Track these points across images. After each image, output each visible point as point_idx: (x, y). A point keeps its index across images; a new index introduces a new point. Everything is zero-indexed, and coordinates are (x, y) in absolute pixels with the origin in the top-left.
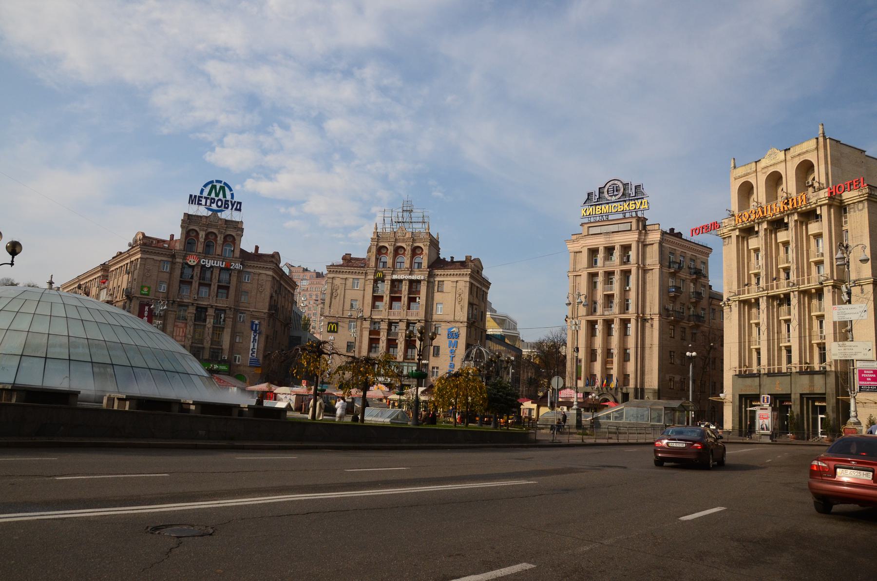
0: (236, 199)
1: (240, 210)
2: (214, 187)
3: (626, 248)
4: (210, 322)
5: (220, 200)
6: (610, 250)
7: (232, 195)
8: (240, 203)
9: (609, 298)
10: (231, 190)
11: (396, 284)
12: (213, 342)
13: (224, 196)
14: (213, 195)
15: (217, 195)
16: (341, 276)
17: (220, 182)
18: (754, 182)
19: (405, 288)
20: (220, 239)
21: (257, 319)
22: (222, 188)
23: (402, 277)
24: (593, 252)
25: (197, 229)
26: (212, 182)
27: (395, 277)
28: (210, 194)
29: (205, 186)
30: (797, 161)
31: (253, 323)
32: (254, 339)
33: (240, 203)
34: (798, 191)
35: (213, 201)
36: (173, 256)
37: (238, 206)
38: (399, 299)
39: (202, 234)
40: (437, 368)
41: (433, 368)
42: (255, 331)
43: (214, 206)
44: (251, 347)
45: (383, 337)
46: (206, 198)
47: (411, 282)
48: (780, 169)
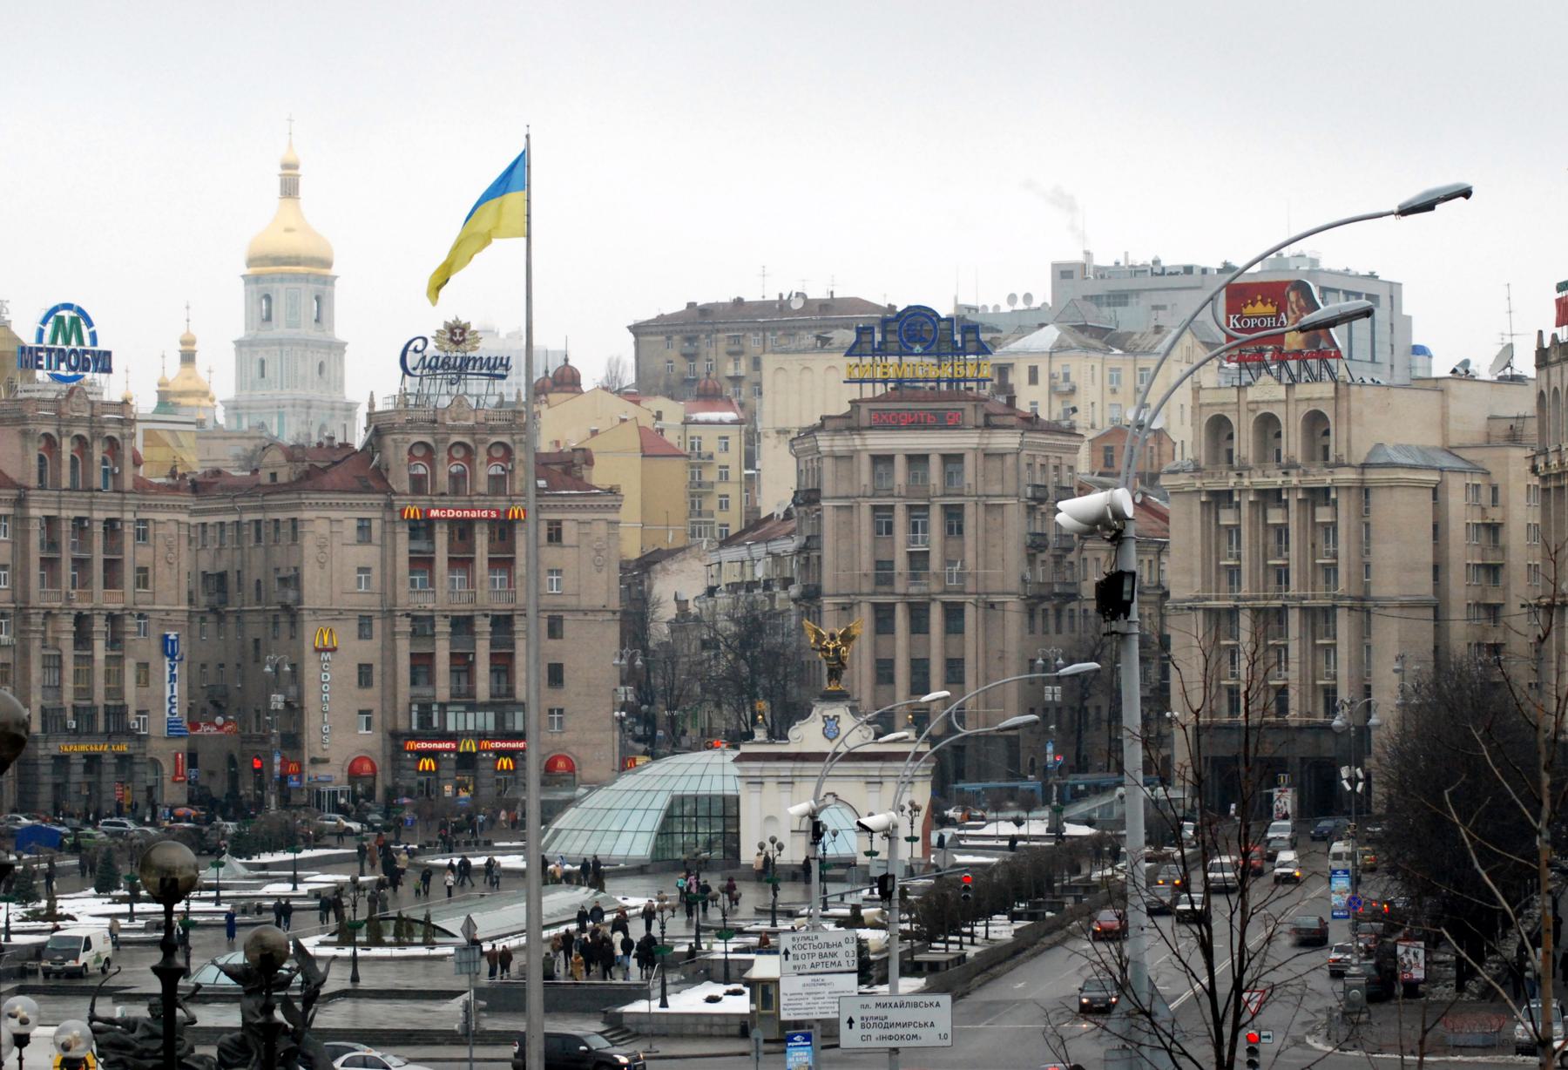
0: (102, 346)
1: (108, 370)
2: (60, 320)
3: (952, 460)
5: (74, 351)
7: (93, 336)
8: (108, 354)
9: (918, 561)
10: (90, 324)
12: (109, 693)
13: (81, 342)
14: (60, 344)
15: (68, 342)
16: (334, 515)
17: (68, 307)
18: (1233, 419)
19: (482, 541)
20: (98, 451)
21: (172, 628)
22: (74, 321)
24: (882, 460)
25: (51, 430)
26: (56, 309)
28: (54, 341)
29: (44, 322)
30: (1304, 409)
31: (166, 637)
32: (173, 677)
33: (108, 354)
35: (62, 356)
36: (21, 502)
37: (103, 362)
39: (67, 448)
40: (560, 711)
41: (551, 711)
42: (172, 659)
43: (63, 370)
44: (168, 694)
46: (50, 351)
48: (1278, 411)
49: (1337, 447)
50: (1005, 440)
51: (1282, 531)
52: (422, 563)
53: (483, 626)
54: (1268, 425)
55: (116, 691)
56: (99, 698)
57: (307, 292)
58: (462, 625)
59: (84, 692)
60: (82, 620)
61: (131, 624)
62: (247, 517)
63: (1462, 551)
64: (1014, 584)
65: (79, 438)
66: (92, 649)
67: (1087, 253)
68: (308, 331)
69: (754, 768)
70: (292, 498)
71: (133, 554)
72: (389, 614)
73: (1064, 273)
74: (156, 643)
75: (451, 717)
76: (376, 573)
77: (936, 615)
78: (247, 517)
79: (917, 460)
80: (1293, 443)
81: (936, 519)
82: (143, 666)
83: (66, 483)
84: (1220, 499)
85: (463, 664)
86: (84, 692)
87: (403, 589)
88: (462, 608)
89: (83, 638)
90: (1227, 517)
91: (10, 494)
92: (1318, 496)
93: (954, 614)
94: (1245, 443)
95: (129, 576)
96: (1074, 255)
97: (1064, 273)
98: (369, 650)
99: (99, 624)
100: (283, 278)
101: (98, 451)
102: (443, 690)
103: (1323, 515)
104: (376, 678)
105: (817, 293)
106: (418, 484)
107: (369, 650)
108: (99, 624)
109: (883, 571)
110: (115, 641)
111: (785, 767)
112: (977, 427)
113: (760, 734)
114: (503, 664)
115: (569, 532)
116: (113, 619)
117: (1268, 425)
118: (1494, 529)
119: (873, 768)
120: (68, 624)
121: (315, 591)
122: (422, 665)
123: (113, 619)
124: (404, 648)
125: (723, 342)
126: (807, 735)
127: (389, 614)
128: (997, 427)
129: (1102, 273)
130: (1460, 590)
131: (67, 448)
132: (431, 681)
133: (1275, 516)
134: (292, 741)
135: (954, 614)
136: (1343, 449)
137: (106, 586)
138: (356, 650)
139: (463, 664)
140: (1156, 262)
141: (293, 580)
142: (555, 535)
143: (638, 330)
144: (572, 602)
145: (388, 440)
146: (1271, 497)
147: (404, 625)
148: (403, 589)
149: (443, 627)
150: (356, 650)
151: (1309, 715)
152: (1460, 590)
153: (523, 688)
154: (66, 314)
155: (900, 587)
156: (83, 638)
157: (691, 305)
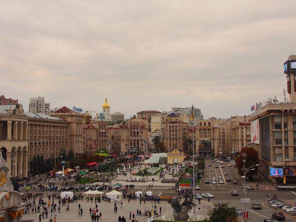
3: (176, 126)
4: (104, 142)
6: (173, 126)
9: (173, 135)
11: (134, 132)
18: (202, 123)
19: (136, 133)
20: (104, 125)
23: (136, 131)
24: (170, 126)
27: (134, 131)
30: (209, 122)
34: (209, 126)
35: (101, 117)
36: (97, 130)
38: (135, 135)
39: (101, 125)
45: (133, 143)
47: (137, 132)
49: (211, 125)
50: (181, 124)
51: (206, 132)
52: (131, 135)
53: (136, 141)
54: (205, 124)
55: (105, 147)
56: (104, 147)
57: (108, 110)
58: (134, 140)
59: (103, 147)
60: (103, 140)
61: (106, 141)
62: (116, 131)
63: (221, 134)
64: (181, 137)
65: (102, 125)
68: (108, 113)
69: (169, 155)
70: (119, 130)
71: (107, 134)
72: (128, 140)
74: (109, 143)
75: (134, 148)
76: (127, 136)
77: (175, 139)
78: (116, 131)
79: (173, 126)
80: (207, 125)
81: (175, 131)
82: (107, 144)
83: (101, 128)
84: (200, 130)
85: (134, 144)
86: (103, 147)
87: (129, 137)
88: (134, 138)
89: (103, 142)
90: (201, 131)
91: (96, 130)
92: (209, 129)
93: (176, 139)
94: (203, 125)
95: (106, 136)
96: (174, 107)
98: (126, 142)
99: (104, 141)
100: (106, 108)
101: (104, 125)
102: (133, 147)
103: (210, 131)
104: (127, 145)
105: (152, 110)
106: (131, 128)
107: (126, 142)
108: (104, 141)
109: (170, 135)
110: (105, 142)
111: (171, 155)
113: (169, 152)
114: (138, 144)
115: (143, 132)
116: (105, 140)
117: (205, 124)
118: (224, 132)
119: (179, 155)
120: (101, 141)
121: (122, 138)
122: (131, 144)
123: (105, 140)
124: (130, 143)
125: (144, 114)
127: (128, 140)
129: (176, 108)
130: (221, 138)
131: (101, 125)
132: (132, 146)
133: (206, 131)
134: (120, 151)
135: (176, 139)
137: (105, 137)
138: (126, 142)
139: (134, 144)
141: (120, 137)
142: (142, 132)
144: (144, 138)
145: (128, 124)
146: (205, 130)
147: (130, 141)
148: (129, 137)
149: (133, 141)
150: (126, 142)
152: (221, 138)
153: (140, 146)
154: (101, 114)
155: (172, 137)
156: (103, 142)
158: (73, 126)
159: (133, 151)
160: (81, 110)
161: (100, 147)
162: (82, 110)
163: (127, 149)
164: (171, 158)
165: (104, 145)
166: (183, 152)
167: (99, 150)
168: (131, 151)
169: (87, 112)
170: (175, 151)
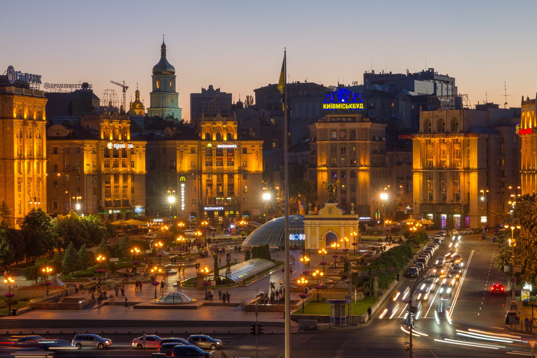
18: (431, 120)
48: (444, 118)
66: (118, 183)
67: (373, 71)
70: (174, 142)
73: (367, 76)
97: (367, 76)
112: (359, 122)
119: (342, 222)
126: (323, 213)
128: (364, 122)
136: (462, 128)
140: (391, 73)
142: (245, 151)
143: (256, 91)
151: (452, 201)
157: (270, 85)
158: (8, 129)
159: (217, 209)
160: (37, 79)
161: (107, 196)
162: (42, 79)
163: (197, 202)
164: (318, 229)
165: (121, 189)
166: (353, 212)
167: (103, 205)
168: (210, 208)
169: (85, 85)
170: (330, 211)
